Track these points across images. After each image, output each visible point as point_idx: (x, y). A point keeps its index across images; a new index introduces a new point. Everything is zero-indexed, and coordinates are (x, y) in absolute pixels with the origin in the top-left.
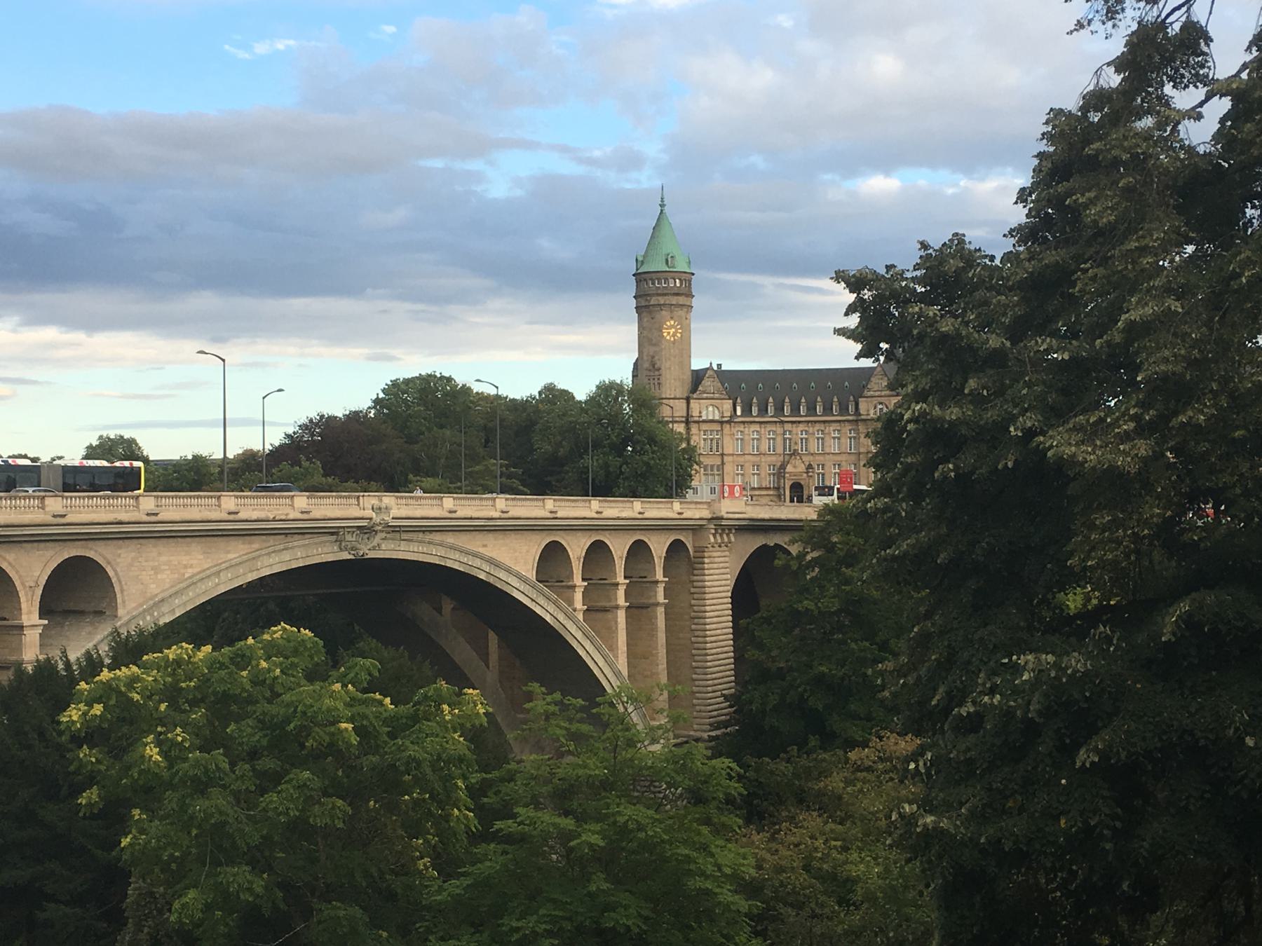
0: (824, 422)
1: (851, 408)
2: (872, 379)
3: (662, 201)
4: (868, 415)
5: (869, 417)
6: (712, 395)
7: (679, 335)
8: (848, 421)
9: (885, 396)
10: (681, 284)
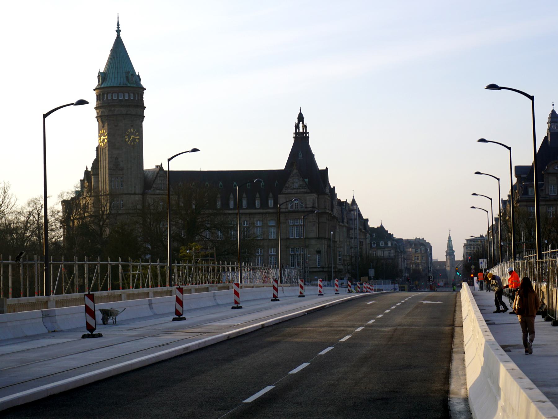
0: (250, 214)
1: (271, 203)
2: (290, 180)
3: (118, 28)
4: (287, 208)
5: (287, 210)
6: (162, 192)
7: (137, 140)
8: (269, 213)
9: (301, 193)
10: (135, 97)
